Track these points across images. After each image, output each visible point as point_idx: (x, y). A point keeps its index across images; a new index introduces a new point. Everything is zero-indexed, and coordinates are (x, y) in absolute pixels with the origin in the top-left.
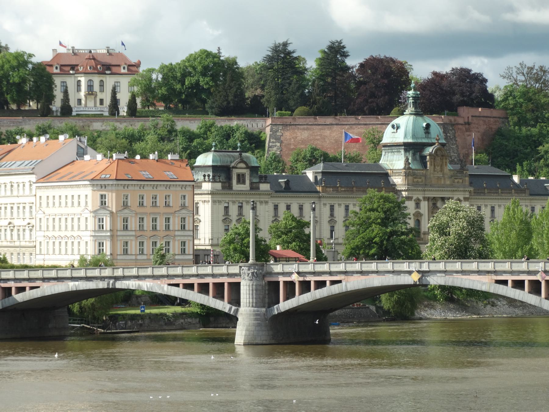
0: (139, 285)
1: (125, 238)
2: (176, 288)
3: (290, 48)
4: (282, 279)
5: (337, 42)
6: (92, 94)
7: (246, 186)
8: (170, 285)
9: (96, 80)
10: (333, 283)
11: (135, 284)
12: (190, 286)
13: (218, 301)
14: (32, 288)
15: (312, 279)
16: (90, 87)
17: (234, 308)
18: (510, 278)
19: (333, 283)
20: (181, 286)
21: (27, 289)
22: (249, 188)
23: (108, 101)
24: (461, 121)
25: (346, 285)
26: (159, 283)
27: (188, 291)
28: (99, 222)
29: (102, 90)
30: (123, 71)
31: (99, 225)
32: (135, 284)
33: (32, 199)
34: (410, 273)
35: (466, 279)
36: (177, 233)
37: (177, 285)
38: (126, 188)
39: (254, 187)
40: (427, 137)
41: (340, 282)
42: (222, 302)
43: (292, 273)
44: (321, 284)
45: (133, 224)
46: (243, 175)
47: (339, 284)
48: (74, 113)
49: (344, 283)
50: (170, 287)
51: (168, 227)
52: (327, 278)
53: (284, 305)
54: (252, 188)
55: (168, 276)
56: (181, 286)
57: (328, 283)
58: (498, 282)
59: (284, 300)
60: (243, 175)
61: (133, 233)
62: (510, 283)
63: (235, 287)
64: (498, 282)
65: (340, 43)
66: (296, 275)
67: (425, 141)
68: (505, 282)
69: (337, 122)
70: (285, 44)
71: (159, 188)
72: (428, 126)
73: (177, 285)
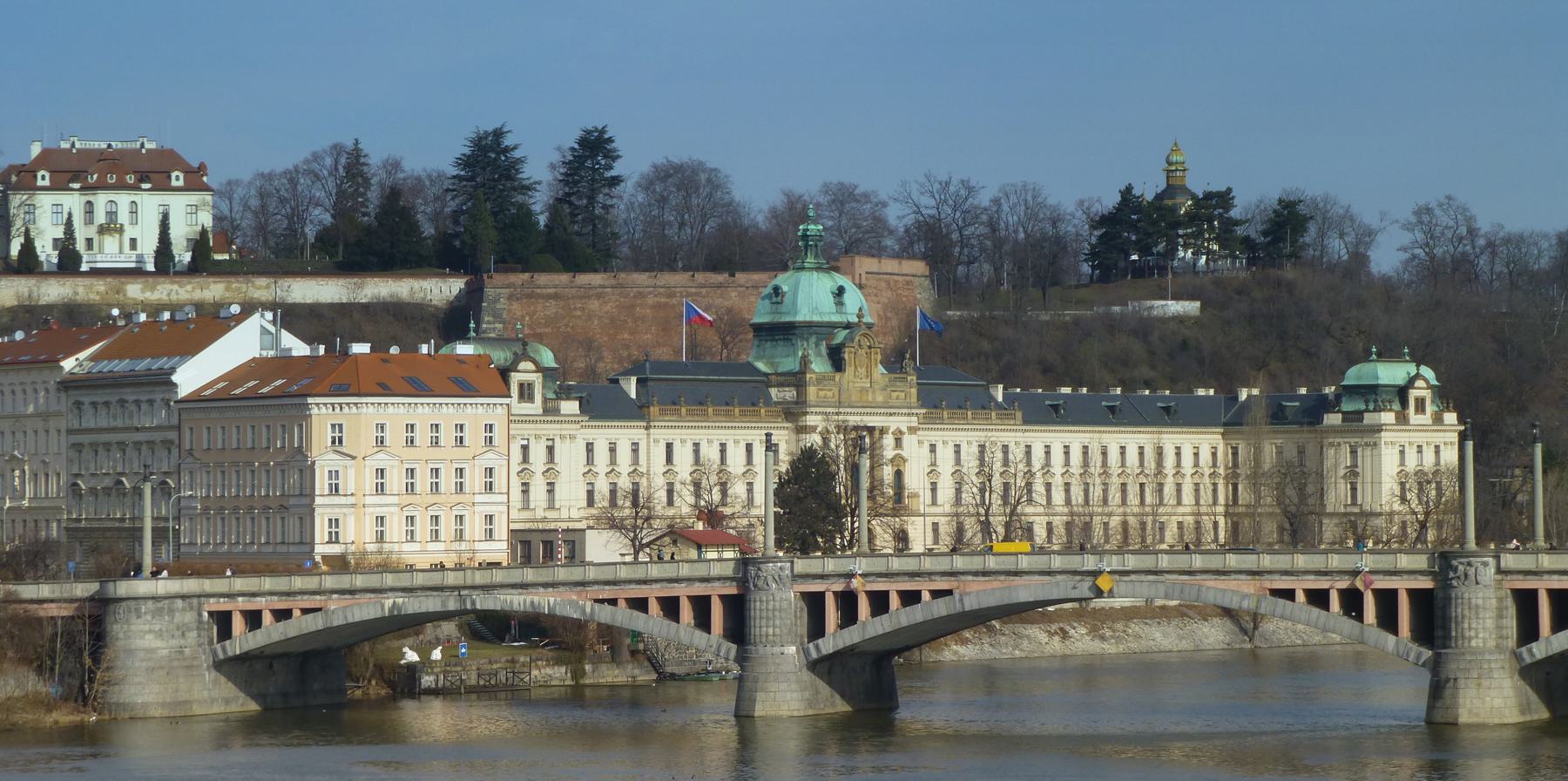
1: (378, 509)
2: (608, 608)
3: (508, 141)
5: (596, 130)
6: (115, 230)
7: (536, 407)
9: (123, 199)
10: (936, 594)
11: (525, 601)
12: (640, 604)
14: (305, 611)
15: (893, 587)
16: (112, 215)
18: (1300, 585)
21: (296, 613)
22: (540, 411)
23: (149, 246)
26: (574, 597)
27: (636, 613)
29: (134, 222)
30: (174, 183)
31: (330, 485)
32: (525, 601)
33: (172, 435)
34: (1096, 574)
36: (478, 498)
37: (613, 602)
39: (550, 410)
41: (949, 592)
42: (705, 635)
44: (911, 598)
45: (395, 481)
46: (530, 385)
47: (947, 598)
48: (84, 267)
49: (957, 596)
50: (597, 606)
51: (460, 487)
52: (925, 587)
53: (834, 639)
54: (546, 411)
57: (926, 596)
60: (530, 385)
61: (395, 500)
62: (1300, 597)
64: (1277, 593)
67: (836, 318)
70: (498, 134)
73: (613, 602)
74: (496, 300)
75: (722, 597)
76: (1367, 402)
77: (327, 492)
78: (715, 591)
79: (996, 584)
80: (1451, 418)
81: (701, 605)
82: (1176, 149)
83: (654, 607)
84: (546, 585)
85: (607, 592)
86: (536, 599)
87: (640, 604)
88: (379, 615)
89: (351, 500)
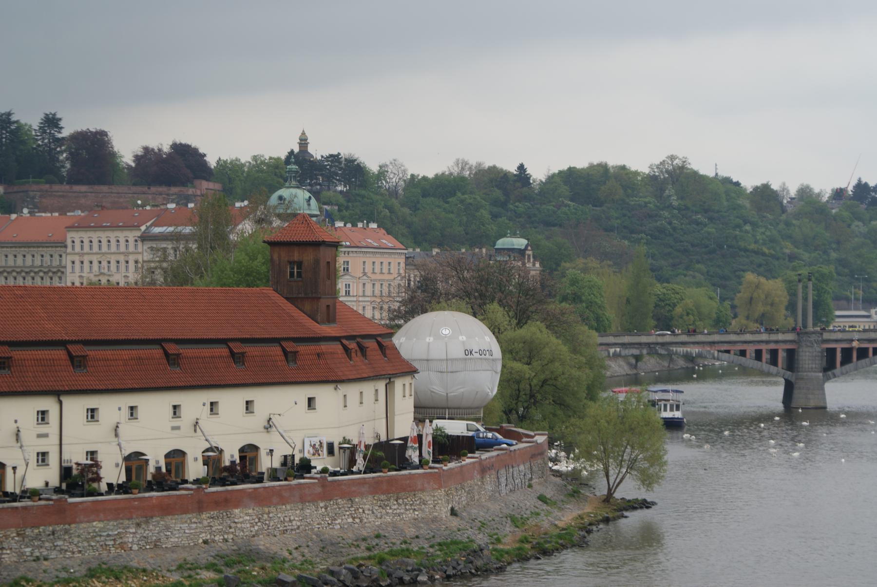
0: (687, 351)
1: (364, 303)
2: (727, 355)
8: (721, 351)
11: (683, 350)
13: (772, 367)
24: (199, 193)
26: (709, 349)
28: (346, 287)
31: (346, 291)
32: (683, 350)
38: (347, 255)
40: (309, 209)
42: (775, 368)
43: (852, 340)
50: (720, 353)
55: (718, 343)
56: (732, 352)
63: (791, 355)
65: (54, 115)
66: (857, 342)
69: (91, 190)
71: (351, 255)
72: (310, 198)
73: (728, 352)
74: (34, 198)
75: (783, 350)
76: (509, 256)
77: (344, 294)
78: (781, 347)
80: (537, 265)
81: (774, 353)
82: (303, 133)
84: (694, 343)
85: (725, 347)
86: (689, 350)
89: (355, 299)
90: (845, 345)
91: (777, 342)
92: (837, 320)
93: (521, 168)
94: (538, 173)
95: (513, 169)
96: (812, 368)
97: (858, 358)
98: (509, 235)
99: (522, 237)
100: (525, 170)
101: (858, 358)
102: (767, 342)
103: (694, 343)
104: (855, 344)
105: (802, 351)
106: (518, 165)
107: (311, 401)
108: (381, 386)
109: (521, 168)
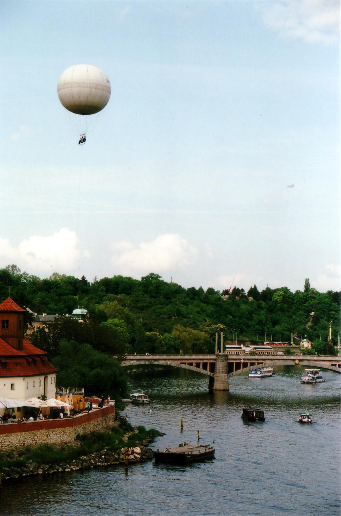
2: (184, 365)
4: (235, 362)
8: (181, 363)
10: (258, 363)
12: (191, 364)
17: (212, 374)
19: (258, 363)
20: (187, 364)
25: (265, 365)
35: (318, 363)
41: (262, 363)
47: (261, 364)
49: (263, 363)
56: (187, 364)
57: (256, 364)
58: (332, 365)
59: (236, 370)
62: (337, 366)
64: (332, 365)
68: (335, 365)
73: (185, 363)
76: (79, 318)
79: (272, 362)
83: (194, 364)
84: (169, 360)
85: (184, 361)
87: (191, 364)
88: (130, 365)
90: (238, 361)
91: (207, 359)
92: (227, 349)
93: (83, 277)
94: (90, 280)
95: (80, 279)
96: (223, 372)
97: (243, 367)
98: (79, 308)
99: (84, 309)
100: (85, 278)
101: (243, 367)
102: (203, 359)
103: (169, 360)
104: (242, 361)
105: (218, 364)
106: (82, 276)
107: (12, 385)
108: (42, 378)
109: (83, 277)
